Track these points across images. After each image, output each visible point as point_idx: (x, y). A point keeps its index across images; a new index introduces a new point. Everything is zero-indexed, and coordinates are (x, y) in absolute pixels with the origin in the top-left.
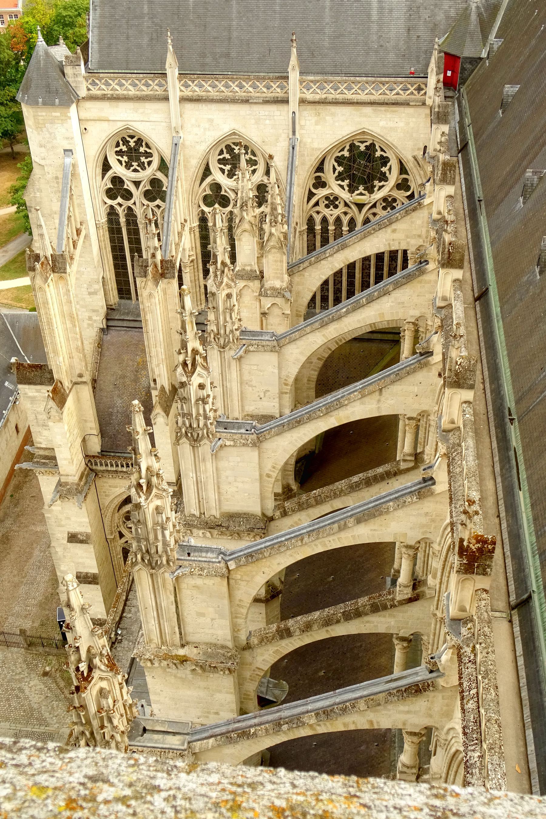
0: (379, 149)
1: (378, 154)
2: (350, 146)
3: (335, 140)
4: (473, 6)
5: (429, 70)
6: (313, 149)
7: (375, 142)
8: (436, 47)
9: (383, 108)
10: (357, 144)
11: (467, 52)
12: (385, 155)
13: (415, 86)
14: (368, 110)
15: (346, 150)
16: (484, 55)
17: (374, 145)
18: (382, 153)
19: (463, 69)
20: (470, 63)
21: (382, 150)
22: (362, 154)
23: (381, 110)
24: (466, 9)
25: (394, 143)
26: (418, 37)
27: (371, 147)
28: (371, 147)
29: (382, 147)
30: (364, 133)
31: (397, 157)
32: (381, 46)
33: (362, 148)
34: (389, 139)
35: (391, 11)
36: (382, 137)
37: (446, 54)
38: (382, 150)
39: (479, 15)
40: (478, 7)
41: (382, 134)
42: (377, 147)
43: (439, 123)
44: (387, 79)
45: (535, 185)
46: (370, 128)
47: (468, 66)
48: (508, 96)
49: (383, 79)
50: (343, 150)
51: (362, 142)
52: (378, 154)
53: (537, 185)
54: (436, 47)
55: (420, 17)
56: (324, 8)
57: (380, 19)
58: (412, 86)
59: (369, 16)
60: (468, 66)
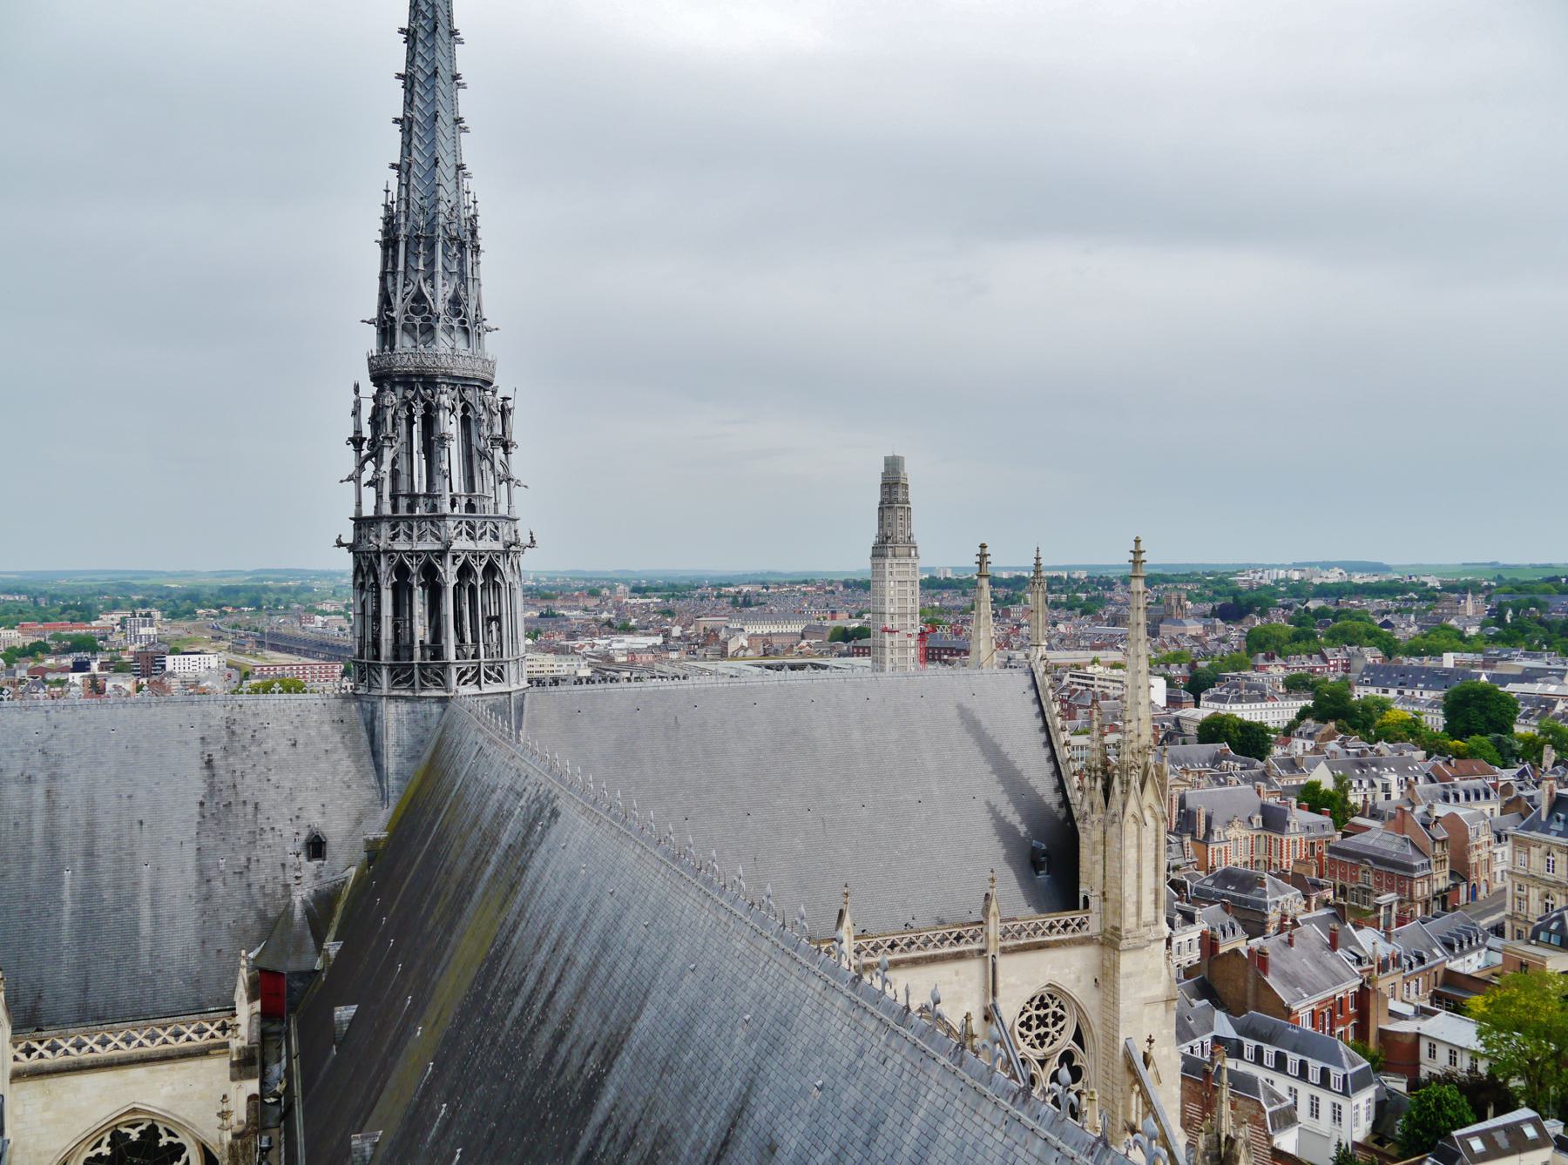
0: (164, 1134)
1: (164, 1141)
2: (112, 1136)
3: (80, 1132)
4: (297, 901)
5: (237, 998)
6: (39, 1155)
7: (156, 1123)
8: (243, 962)
9: (165, 1067)
10: (124, 1130)
11: (290, 965)
12: (175, 1141)
13: (217, 1024)
14: (139, 1072)
15: (104, 1144)
16: (319, 965)
17: (156, 1128)
18: (171, 1139)
19: (291, 990)
20: (300, 980)
21: (170, 1133)
22: (135, 1147)
23: (161, 1070)
24: (288, 905)
25: (189, 1119)
26: (219, 951)
27: (152, 1133)
28: (152, 1133)
29: (170, 1128)
30: (134, 1111)
31: (197, 1141)
32: (159, 971)
33: (134, 1135)
34: (180, 1113)
35: (172, 918)
36: (168, 1112)
37: (262, 971)
38: (170, 1133)
39: (308, 912)
40: (304, 902)
41: (165, 1108)
42: (161, 1131)
43: (242, 1079)
44: (168, 1020)
45: (368, 1158)
46: (145, 1101)
47: (297, 984)
48: (341, 1023)
49: (163, 1020)
50: (98, 1145)
51: (134, 1127)
52: (164, 1141)
53: (372, 1157)
54: (243, 962)
55: (220, 923)
56: (58, 925)
57: (155, 930)
58: (212, 1025)
59: (136, 931)
60: (297, 984)
